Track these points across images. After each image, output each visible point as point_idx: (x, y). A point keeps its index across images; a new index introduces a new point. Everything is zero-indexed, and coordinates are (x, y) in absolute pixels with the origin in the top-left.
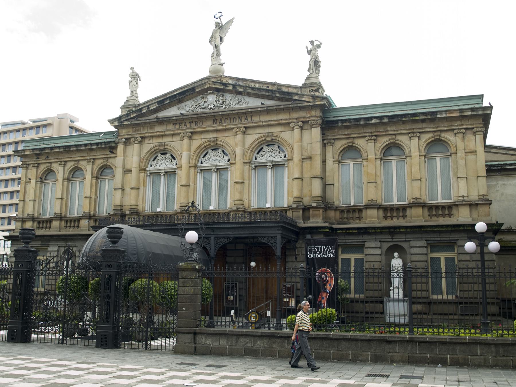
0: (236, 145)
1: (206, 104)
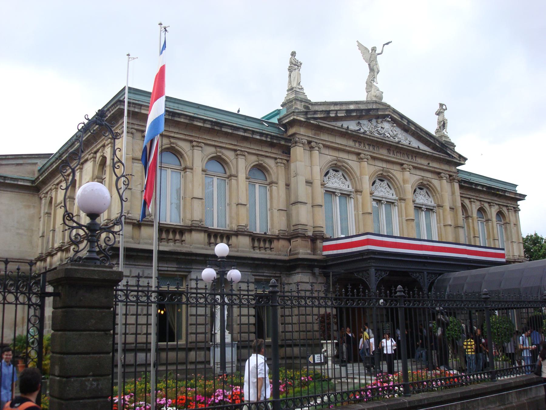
0: (405, 181)
1: (383, 131)
